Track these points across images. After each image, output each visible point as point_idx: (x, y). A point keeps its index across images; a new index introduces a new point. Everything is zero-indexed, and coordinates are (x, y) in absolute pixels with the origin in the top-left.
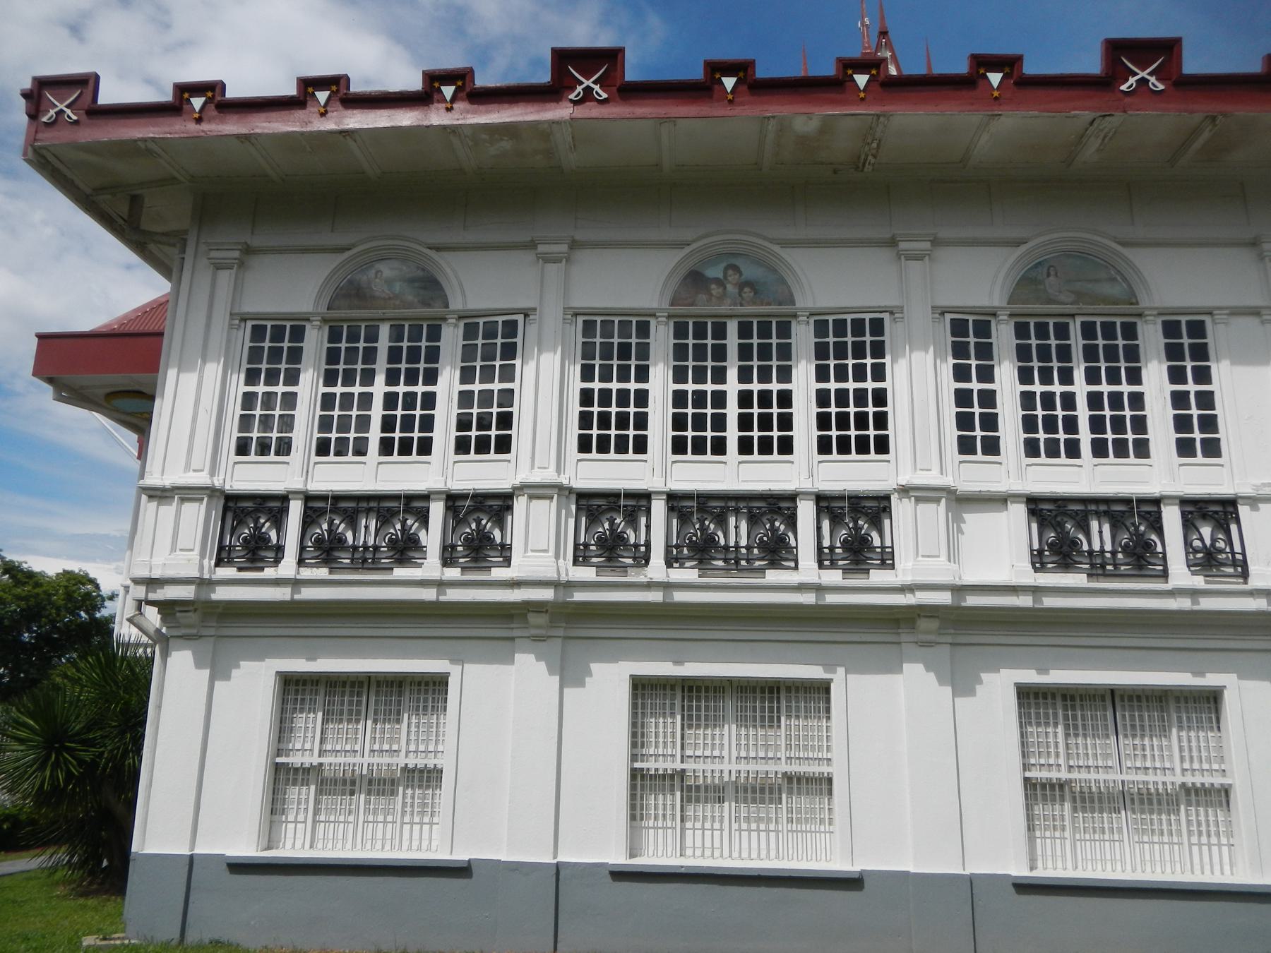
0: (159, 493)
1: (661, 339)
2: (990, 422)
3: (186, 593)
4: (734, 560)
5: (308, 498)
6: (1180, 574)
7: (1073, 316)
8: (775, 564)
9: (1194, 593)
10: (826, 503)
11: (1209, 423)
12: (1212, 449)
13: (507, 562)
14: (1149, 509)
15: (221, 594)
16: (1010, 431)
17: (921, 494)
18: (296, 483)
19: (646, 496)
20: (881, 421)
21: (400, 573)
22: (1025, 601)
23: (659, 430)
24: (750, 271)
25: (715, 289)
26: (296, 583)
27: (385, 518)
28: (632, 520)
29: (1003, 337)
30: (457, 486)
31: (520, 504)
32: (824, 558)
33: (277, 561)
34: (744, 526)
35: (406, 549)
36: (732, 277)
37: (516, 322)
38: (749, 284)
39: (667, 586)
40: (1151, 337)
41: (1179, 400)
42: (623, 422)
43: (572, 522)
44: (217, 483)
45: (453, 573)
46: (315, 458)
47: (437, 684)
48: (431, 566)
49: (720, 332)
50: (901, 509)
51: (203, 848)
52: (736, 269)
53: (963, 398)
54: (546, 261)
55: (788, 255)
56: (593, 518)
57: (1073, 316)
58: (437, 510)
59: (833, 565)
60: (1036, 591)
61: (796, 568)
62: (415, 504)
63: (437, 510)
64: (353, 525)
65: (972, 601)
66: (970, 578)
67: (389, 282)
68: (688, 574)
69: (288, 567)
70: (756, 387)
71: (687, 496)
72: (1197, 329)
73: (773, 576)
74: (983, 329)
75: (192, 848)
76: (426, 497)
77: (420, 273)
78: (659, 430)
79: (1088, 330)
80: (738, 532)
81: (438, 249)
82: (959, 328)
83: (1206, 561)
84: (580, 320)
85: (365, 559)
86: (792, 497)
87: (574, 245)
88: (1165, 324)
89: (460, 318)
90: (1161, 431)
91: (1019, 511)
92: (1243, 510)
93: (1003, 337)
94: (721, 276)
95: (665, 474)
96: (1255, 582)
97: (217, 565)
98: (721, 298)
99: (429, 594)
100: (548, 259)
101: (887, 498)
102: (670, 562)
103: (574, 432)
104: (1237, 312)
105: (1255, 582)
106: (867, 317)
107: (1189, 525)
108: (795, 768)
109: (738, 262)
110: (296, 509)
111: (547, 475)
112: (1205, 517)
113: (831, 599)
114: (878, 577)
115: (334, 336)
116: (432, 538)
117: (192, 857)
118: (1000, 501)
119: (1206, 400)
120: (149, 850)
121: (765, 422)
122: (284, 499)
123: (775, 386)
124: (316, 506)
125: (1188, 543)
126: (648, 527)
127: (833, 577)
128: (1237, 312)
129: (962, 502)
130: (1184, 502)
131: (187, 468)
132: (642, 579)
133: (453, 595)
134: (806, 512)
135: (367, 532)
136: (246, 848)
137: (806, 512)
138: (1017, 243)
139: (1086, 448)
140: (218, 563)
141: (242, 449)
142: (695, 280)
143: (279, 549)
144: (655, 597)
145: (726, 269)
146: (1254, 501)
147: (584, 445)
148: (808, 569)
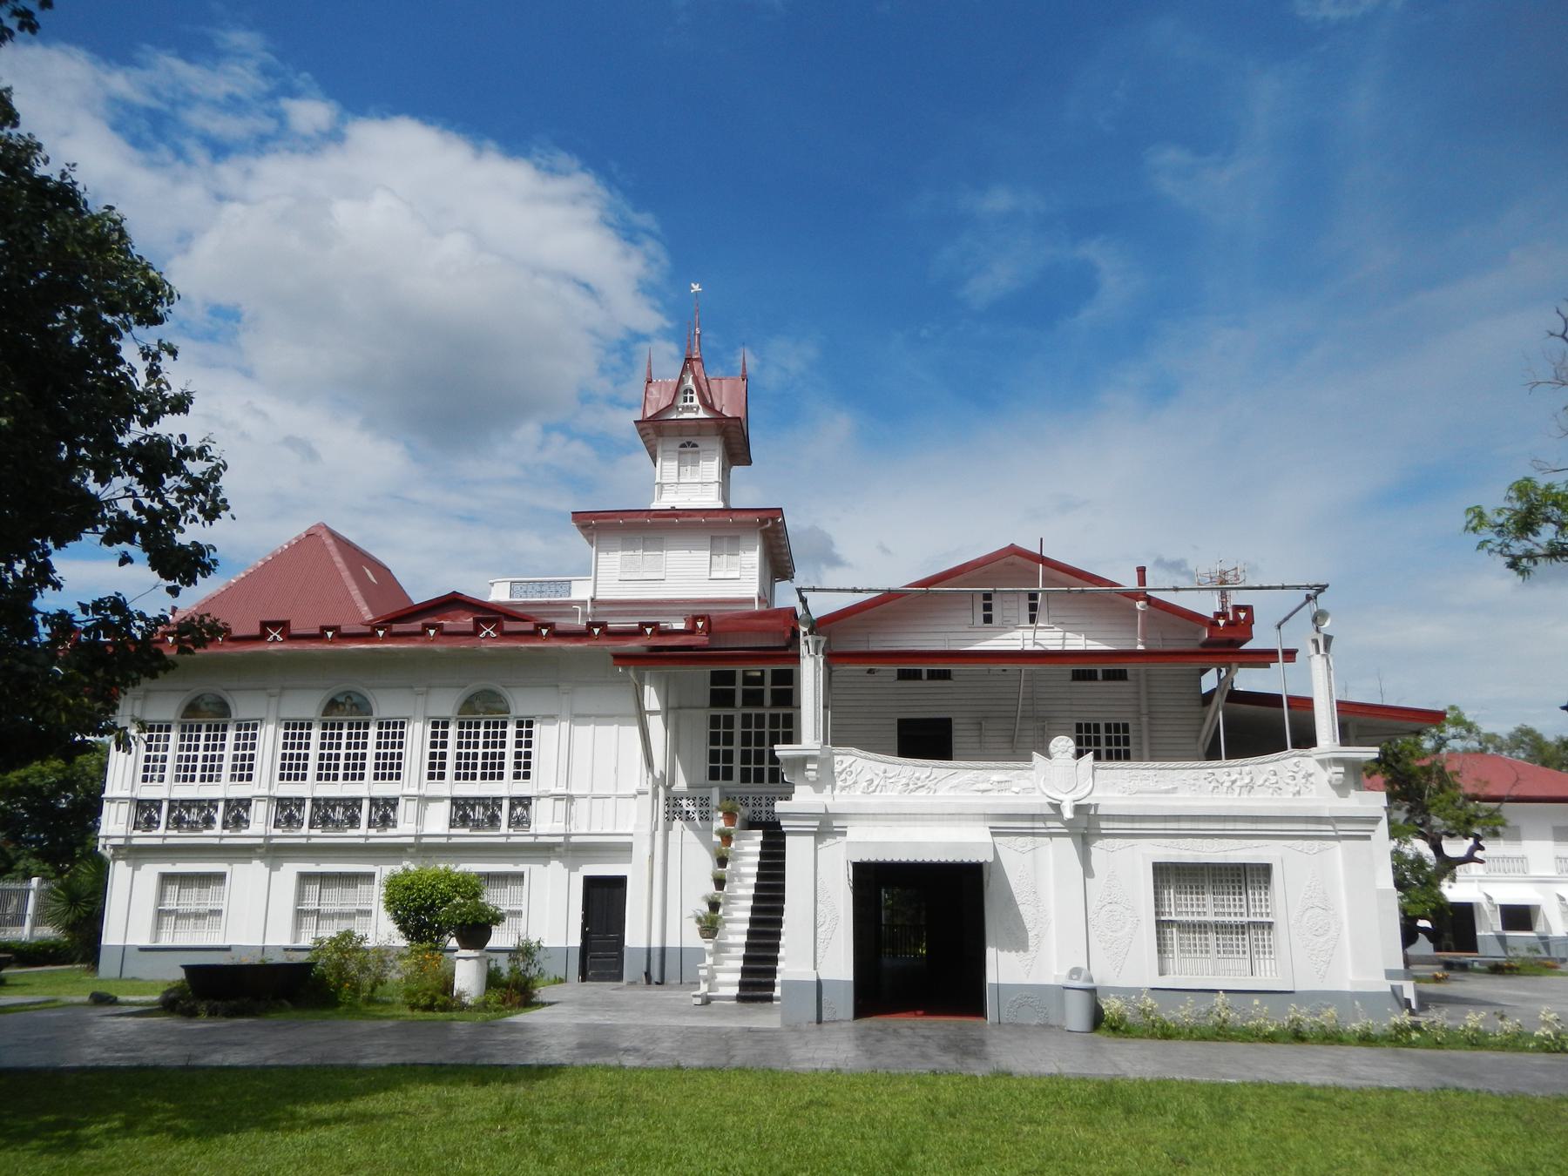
2: (443, 766)
3: (121, 841)
4: (338, 825)
5: (171, 801)
6: (504, 828)
9: (508, 836)
10: (374, 801)
11: (528, 765)
12: (527, 776)
14: (497, 801)
15: (135, 841)
16: (450, 770)
17: (409, 798)
18: (166, 796)
19: (303, 800)
20: (399, 766)
21: (206, 832)
22: (444, 840)
23: (312, 771)
24: (356, 699)
26: (165, 837)
27: (201, 809)
28: (299, 810)
29: (453, 730)
30: (230, 796)
31: (253, 802)
32: (371, 824)
33: (158, 827)
35: (209, 822)
36: (349, 701)
38: (356, 705)
39: (309, 837)
40: (511, 730)
41: (518, 755)
42: (297, 767)
43: (275, 808)
44: (134, 796)
45: (226, 832)
46: (174, 783)
48: (217, 829)
50: (402, 802)
51: (127, 943)
52: (349, 697)
53: (433, 756)
54: (271, 696)
56: (284, 808)
58: (221, 805)
59: (374, 827)
60: (449, 836)
62: (213, 803)
64: (189, 812)
65: (425, 840)
66: (425, 832)
67: (207, 704)
69: (161, 830)
71: (319, 799)
73: (351, 832)
74: (446, 725)
75: (125, 942)
76: (217, 800)
78: (312, 771)
80: (339, 814)
81: (226, 690)
84: (284, 723)
85: (193, 826)
86: (361, 799)
87: (283, 688)
88: (518, 722)
90: (509, 769)
91: (448, 802)
92: (534, 802)
93: (453, 730)
94: (343, 700)
95: (313, 790)
96: (532, 831)
97: (134, 829)
99: (216, 841)
100: (271, 696)
101: (397, 799)
103: (278, 771)
105: (532, 831)
106: (399, 721)
107: (512, 807)
108: (361, 908)
109: (352, 695)
110: (165, 806)
111: (264, 791)
112: (520, 804)
113: (372, 841)
114: (390, 831)
115: (183, 729)
116: (219, 817)
117: (124, 948)
118: (440, 799)
119: (528, 755)
120: (108, 943)
121: (355, 767)
122: (160, 801)
125: (510, 815)
128: (545, 717)
129: (425, 800)
130: (511, 799)
131: (122, 789)
132: (299, 834)
133: (226, 841)
134: (366, 804)
135: (194, 815)
136: (146, 943)
137: (366, 804)
138: (463, 687)
140: (134, 829)
141: (145, 779)
143: (159, 822)
144: (304, 841)
146: (538, 798)
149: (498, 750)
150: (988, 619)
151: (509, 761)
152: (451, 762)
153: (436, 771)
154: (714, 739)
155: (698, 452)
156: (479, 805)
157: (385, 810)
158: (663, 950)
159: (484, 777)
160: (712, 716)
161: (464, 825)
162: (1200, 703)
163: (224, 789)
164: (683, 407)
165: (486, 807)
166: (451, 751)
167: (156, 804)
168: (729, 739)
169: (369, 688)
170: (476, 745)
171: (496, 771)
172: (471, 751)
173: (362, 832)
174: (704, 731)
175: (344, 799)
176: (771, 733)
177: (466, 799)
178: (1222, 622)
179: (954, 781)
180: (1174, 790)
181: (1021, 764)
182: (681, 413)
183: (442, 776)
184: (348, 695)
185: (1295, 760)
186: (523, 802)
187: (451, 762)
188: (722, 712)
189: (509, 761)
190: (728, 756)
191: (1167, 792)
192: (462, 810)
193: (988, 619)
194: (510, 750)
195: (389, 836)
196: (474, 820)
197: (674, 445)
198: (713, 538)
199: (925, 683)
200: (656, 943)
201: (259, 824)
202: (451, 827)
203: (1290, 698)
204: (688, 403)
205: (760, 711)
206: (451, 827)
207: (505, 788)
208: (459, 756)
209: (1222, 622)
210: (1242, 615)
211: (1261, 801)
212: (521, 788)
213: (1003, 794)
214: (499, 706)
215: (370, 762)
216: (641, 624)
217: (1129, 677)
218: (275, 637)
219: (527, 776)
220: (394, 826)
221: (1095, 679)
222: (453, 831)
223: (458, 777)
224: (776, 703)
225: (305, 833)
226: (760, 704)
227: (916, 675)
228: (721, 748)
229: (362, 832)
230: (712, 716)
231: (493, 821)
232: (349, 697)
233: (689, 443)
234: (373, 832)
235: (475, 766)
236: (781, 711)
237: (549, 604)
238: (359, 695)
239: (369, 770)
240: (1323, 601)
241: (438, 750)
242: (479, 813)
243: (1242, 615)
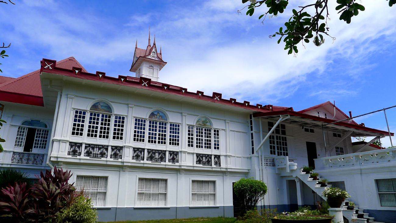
0: (56, 140)
1: (147, 124)
2: (192, 142)
6: (213, 166)
7: (203, 127)
12: (218, 148)
13: (121, 158)
19: (144, 149)
21: (102, 159)
23: (146, 139)
24: (161, 114)
25: (156, 116)
27: (99, 149)
28: (141, 153)
32: (169, 161)
34: (158, 154)
35: (103, 155)
36: (158, 115)
37: (124, 117)
47: (106, 178)
49: (156, 123)
52: (159, 113)
53: (189, 138)
55: (167, 113)
57: (203, 127)
61: (165, 162)
63: (110, 149)
67: (102, 106)
70: (161, 133)
72: (218, 131)
73: (162, 163)
77: (107, 106)
80: (157, 156)
83: (216, 163)
84: (135, 118)
85: (96, 156)
89: (115, 115)
90: (213, 146)
98: (157, 118)
101: (178, 152)
102: (147, 160)
104: (223, 130)
109: (159, 112)
114: (177, 164)
119: (218, 141)
123: (164, 133)
124: (88, 146)
126: (144, 154)
127: (171, 164)
128: (223, 130)
137: (167, 153)
142: (152, 115)
145: (157, 113)
147: (134, 140)
151: (213, 143)
153: (190, 144)
156: (204, 156)
157: (174, 156)
158: (264, 205)
161: (200, 163)
163: (111, 142)
167: (79, 145)
168: (274, 143)
169: (167, 111)
175: (159, 151)
177: (200, 154)
182: (151, 57)
184: (158, 112)
186: (218, 157)
192: (200, 158)
196: (203, 162)
197: (148, 66)
200: (263, 205)
201: (128, 157)
207: (212, 152)
215: (168, 138)
218: (145, 84)
225: (146, 162)
229: (167, 163)
231: (209, 162)
232: (159, 113)
233: (151, 66)
238: (162, 113)
239: (168, 141)
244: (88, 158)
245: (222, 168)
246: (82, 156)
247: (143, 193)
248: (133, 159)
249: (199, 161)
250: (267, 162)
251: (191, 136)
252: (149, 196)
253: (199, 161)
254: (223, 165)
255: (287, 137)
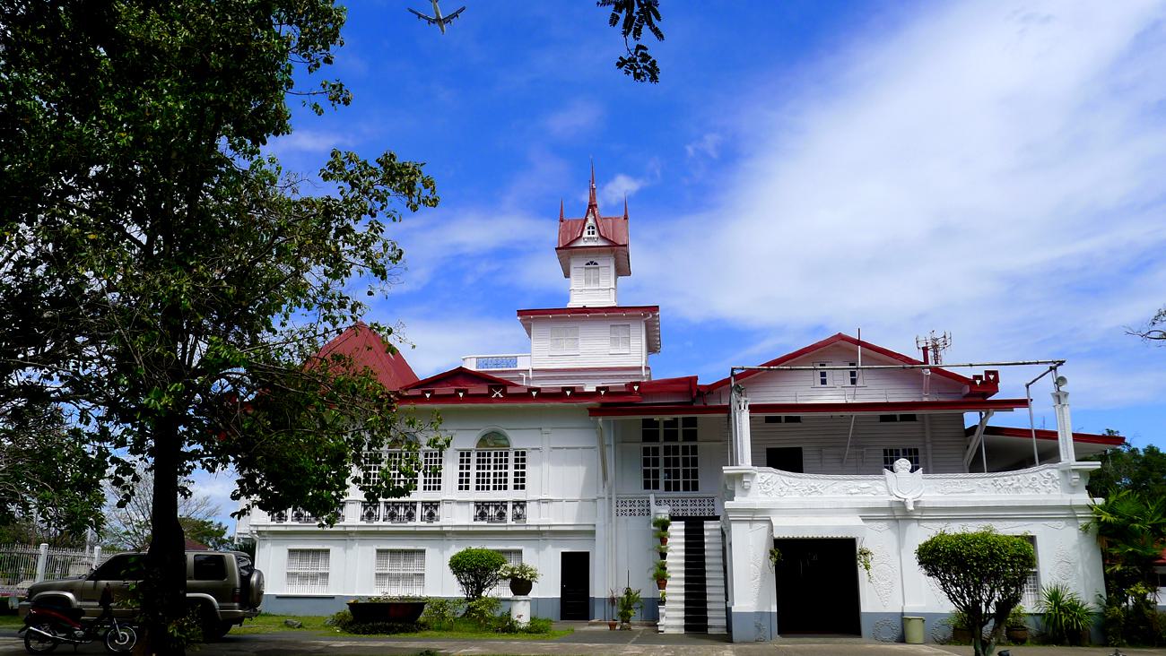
2: (467, 481)
6: (509, 521)
8: (410, 520)
12: (523, 487)
14: (503, 504)
16: (473, 484)
25: (400, 443)
28: (375, 509)
29: (474, 457)
40: (511, 457)
41: (516, 474)
53: (461, 475)
68: (388, 523)
72: (523, 454)
73: (409, 523)
74: (468, 455)
79: (496, 455)
82: (462, 455)
83: (518, 517)
90: (511, 484)
93: (474, 457)
107: (514, 507)
114: (435, 523)
119: (523, 474)
137: (419, 506)
139: (491, 488)
148: (418, 522)
149: (503, 471)
150: (824, 382)
151: (511, 478)
152: (473, 478)
153: (463, 484)
154: (646, 463)
155: (598, 268)
157: (432, 506)
159: (495, 488)
160: (644, 448)
161: (483, 520)
162: (964, 434)
164: (588, 238)
165: (496, 508)
166: (473, 471)
168: (656, 463)
170: (489, 468)
171: (503, 484)
172: (498, 471)
173: (418, 523)
174: (640, 457)
176: (684, 459)
177: (483, 503)
178: (978, 382)
179: (836, 488)
180: (973, 491)
181: (878, 477)
183: (467, 488)
185: (1048, 471)
186: (520, 504)
187: (473, 478)
188: (651, 445)
189: (511, 478)
190: (656, 474)
191: (969, 492)
193: (824, 382)
194: (511, 471)
195: (434, 526)
198: (611, 326)
199: (783, 425)
202: (475, 520)
203: (1035, 431)
204: (591, 236)
205: (675, 444)
206: (475, 520)
207: (510, 495)
208: (478, 475)
209: (978, 382)
210: (992, 377)
211: (1027, 497)
212: (519, 495)
213: (866, 495)
214: (505, 442)
216: (597, 388)
217: (917, 419)
219: (523, 487)
220: (438, 520)
221: (895, 420)
222: (476, 523)
223: (478, 488)
224: (685, 439)
226: (676, 439)
227: (778, 420)
228: (651, 468)
230: (644, 448)
231: (501, 516)
233: (592, 262)
234: (425, 523)
235: (488, 481)
236: (690, 444)
237: (503, 372)
240: (1061, 371)
241: (465, 471)
242: (492, 512)
243: (992, 377)
244: (297, 523)
245: (530, 526)
246: (289, 522)
247: (385, 574)
248: (362, 519)
249: (482, 516)
250: (632, 508)
251: (465, 471)
252: (304, 578)
253: (482, 516)
254: (530, 521)
255: (700, 445)
